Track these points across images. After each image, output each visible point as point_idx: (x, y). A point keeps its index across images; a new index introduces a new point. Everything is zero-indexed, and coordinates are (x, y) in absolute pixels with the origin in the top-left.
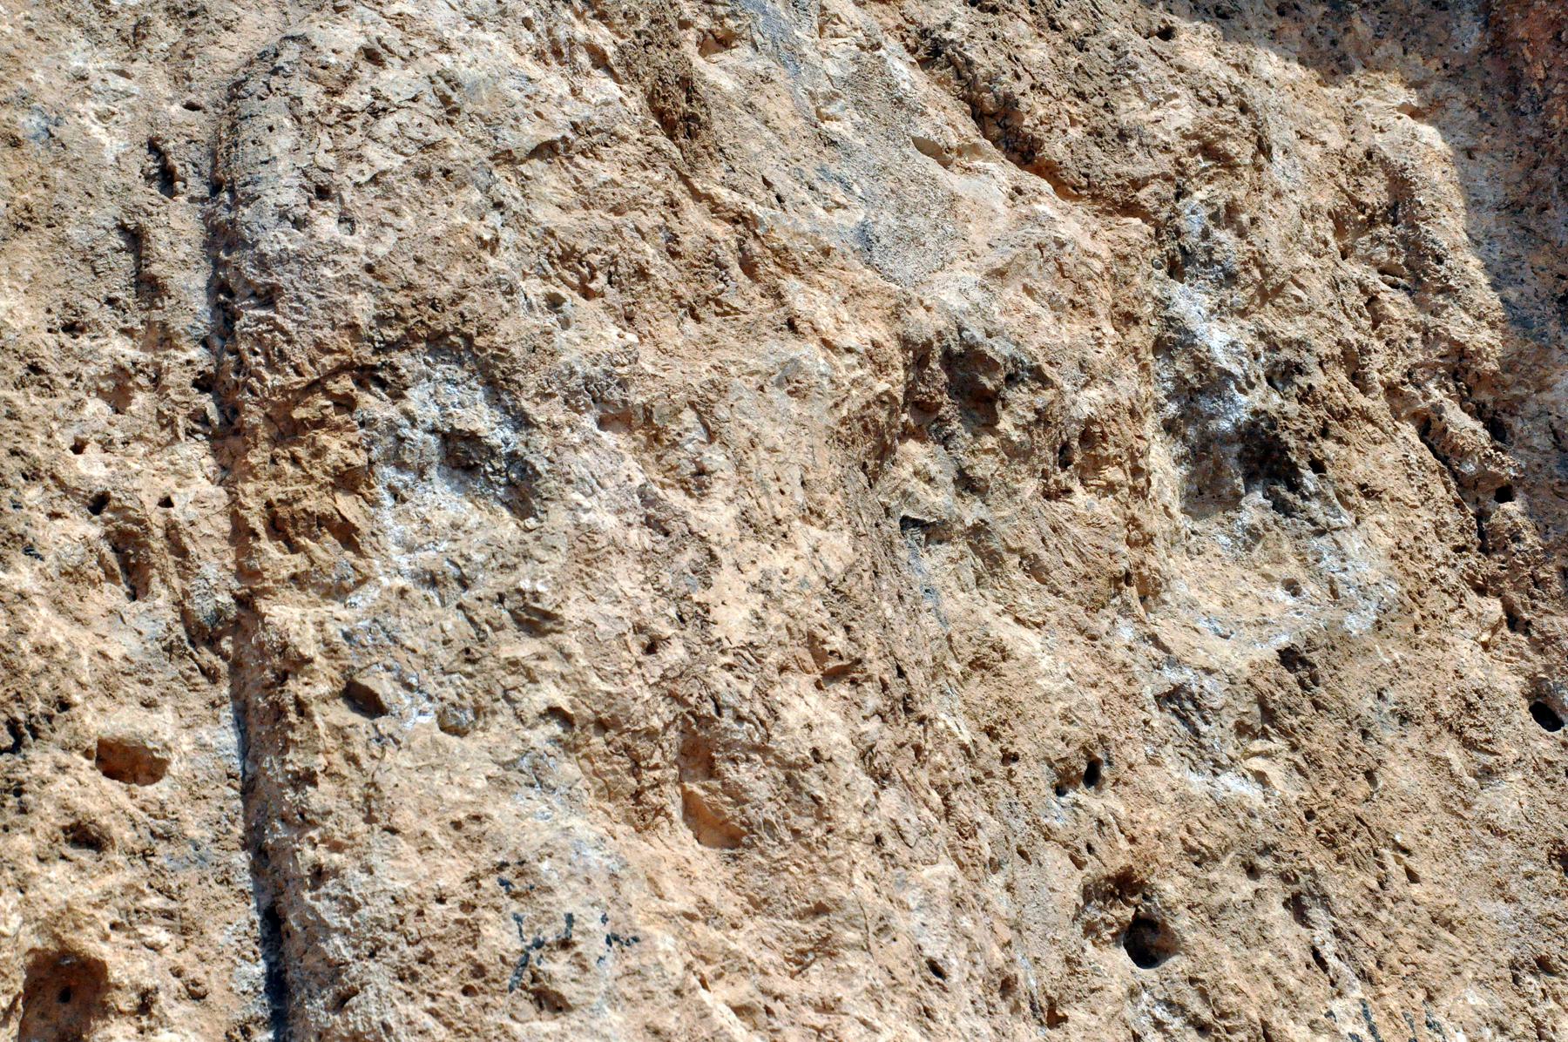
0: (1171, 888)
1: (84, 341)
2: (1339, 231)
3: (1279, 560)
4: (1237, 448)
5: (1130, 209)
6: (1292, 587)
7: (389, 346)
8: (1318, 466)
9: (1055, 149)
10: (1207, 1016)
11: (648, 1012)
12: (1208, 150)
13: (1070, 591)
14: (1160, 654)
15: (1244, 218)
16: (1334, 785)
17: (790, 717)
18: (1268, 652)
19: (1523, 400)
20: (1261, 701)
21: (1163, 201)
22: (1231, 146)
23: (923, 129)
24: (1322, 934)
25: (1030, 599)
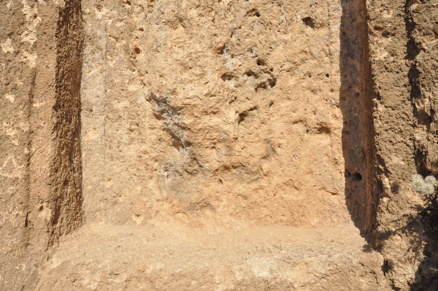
0: (259, 9)
10: (262, 22)
11: (166, 51)
17: (188, 15)
24: (282, 8)
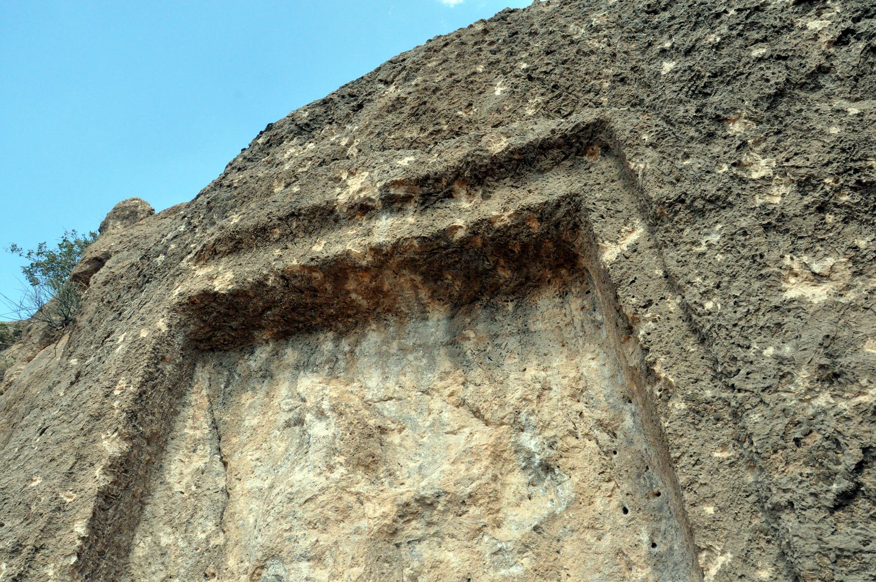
1: (243, 564)
2: (573, 396)
3: (551, 494)
4: (540, 468)
5: (502, 424)
6: (552, 500)
7: (265, 560)
8: (558, 467)
9: (488, 416)
12: (525, 399)
13: (463, 539)
14: (495, 541)
15: (536, 412)
16: (544, 559)
18: (528, 529)
19: (618, 426)
20: (523, 544)
21: (510, 419)
22: (530, 397)
23: (448, 429)
25: (450, 543)
